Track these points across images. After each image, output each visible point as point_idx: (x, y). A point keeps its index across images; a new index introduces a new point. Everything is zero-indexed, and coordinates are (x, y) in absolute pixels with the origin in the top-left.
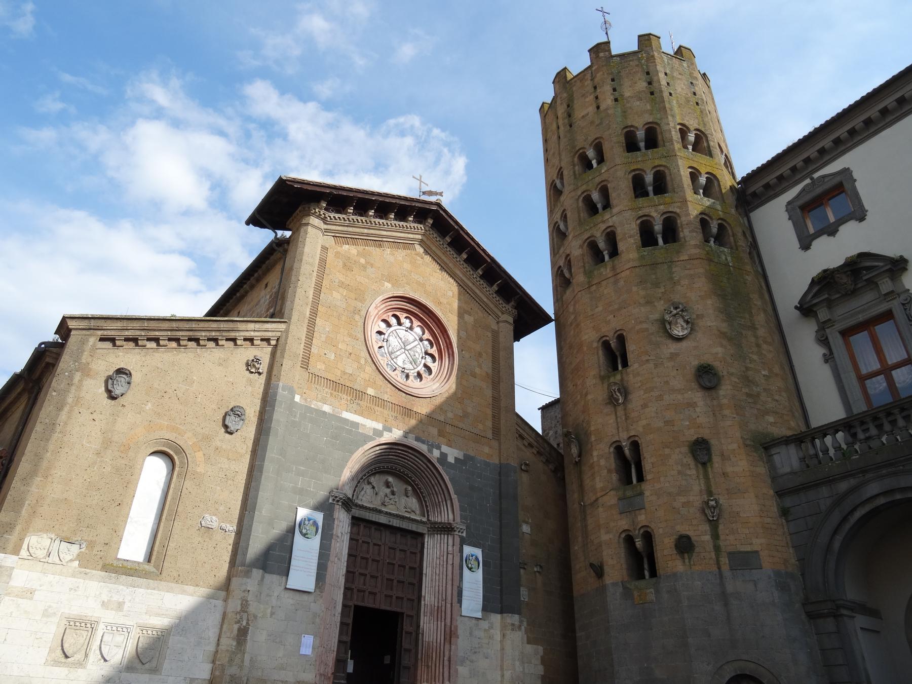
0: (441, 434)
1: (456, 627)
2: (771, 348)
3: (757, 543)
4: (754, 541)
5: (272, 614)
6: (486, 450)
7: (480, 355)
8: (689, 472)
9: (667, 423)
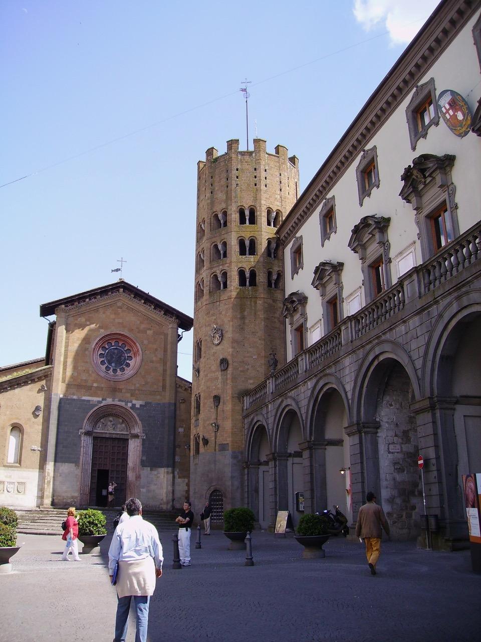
0: (132, 395)
1: (140, 475)
2: (263, 342)
3: (229, 440)
4: (228, 439)
5: (60, 476)
6: (158, 397)
7: (156, 350)
8: (212, 411)
9: (208, 387)
